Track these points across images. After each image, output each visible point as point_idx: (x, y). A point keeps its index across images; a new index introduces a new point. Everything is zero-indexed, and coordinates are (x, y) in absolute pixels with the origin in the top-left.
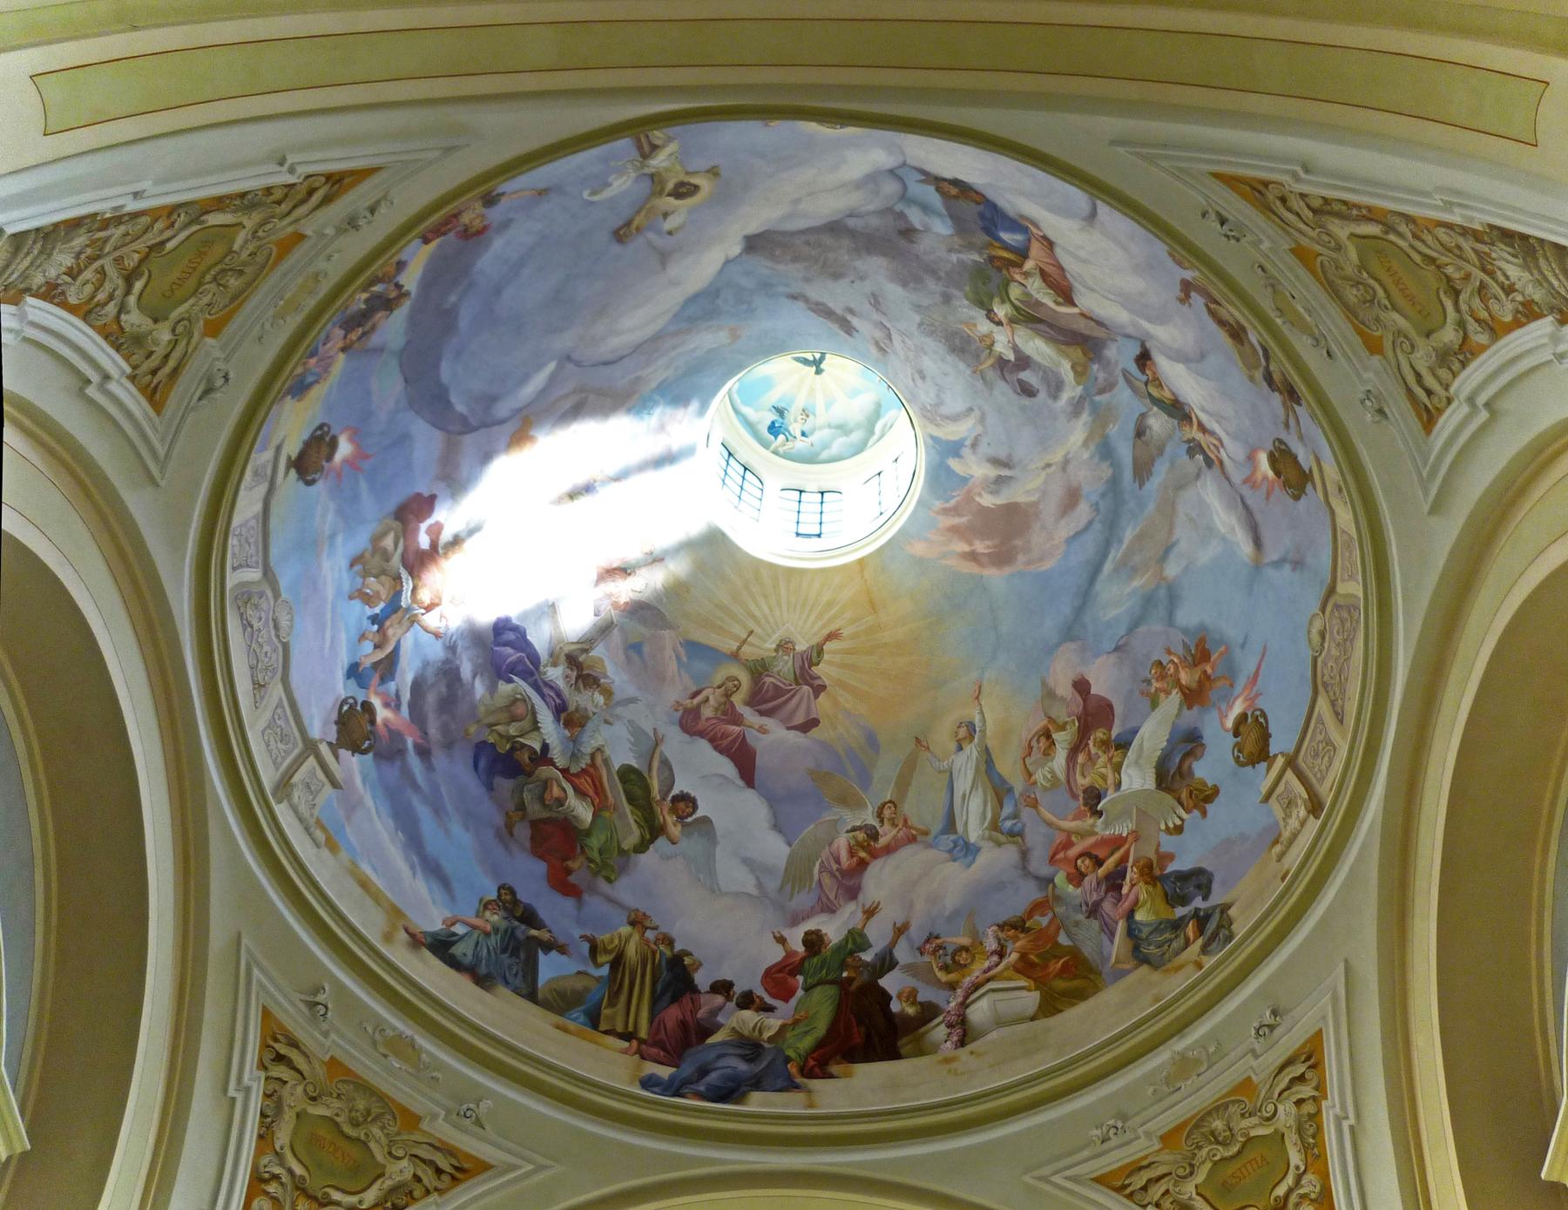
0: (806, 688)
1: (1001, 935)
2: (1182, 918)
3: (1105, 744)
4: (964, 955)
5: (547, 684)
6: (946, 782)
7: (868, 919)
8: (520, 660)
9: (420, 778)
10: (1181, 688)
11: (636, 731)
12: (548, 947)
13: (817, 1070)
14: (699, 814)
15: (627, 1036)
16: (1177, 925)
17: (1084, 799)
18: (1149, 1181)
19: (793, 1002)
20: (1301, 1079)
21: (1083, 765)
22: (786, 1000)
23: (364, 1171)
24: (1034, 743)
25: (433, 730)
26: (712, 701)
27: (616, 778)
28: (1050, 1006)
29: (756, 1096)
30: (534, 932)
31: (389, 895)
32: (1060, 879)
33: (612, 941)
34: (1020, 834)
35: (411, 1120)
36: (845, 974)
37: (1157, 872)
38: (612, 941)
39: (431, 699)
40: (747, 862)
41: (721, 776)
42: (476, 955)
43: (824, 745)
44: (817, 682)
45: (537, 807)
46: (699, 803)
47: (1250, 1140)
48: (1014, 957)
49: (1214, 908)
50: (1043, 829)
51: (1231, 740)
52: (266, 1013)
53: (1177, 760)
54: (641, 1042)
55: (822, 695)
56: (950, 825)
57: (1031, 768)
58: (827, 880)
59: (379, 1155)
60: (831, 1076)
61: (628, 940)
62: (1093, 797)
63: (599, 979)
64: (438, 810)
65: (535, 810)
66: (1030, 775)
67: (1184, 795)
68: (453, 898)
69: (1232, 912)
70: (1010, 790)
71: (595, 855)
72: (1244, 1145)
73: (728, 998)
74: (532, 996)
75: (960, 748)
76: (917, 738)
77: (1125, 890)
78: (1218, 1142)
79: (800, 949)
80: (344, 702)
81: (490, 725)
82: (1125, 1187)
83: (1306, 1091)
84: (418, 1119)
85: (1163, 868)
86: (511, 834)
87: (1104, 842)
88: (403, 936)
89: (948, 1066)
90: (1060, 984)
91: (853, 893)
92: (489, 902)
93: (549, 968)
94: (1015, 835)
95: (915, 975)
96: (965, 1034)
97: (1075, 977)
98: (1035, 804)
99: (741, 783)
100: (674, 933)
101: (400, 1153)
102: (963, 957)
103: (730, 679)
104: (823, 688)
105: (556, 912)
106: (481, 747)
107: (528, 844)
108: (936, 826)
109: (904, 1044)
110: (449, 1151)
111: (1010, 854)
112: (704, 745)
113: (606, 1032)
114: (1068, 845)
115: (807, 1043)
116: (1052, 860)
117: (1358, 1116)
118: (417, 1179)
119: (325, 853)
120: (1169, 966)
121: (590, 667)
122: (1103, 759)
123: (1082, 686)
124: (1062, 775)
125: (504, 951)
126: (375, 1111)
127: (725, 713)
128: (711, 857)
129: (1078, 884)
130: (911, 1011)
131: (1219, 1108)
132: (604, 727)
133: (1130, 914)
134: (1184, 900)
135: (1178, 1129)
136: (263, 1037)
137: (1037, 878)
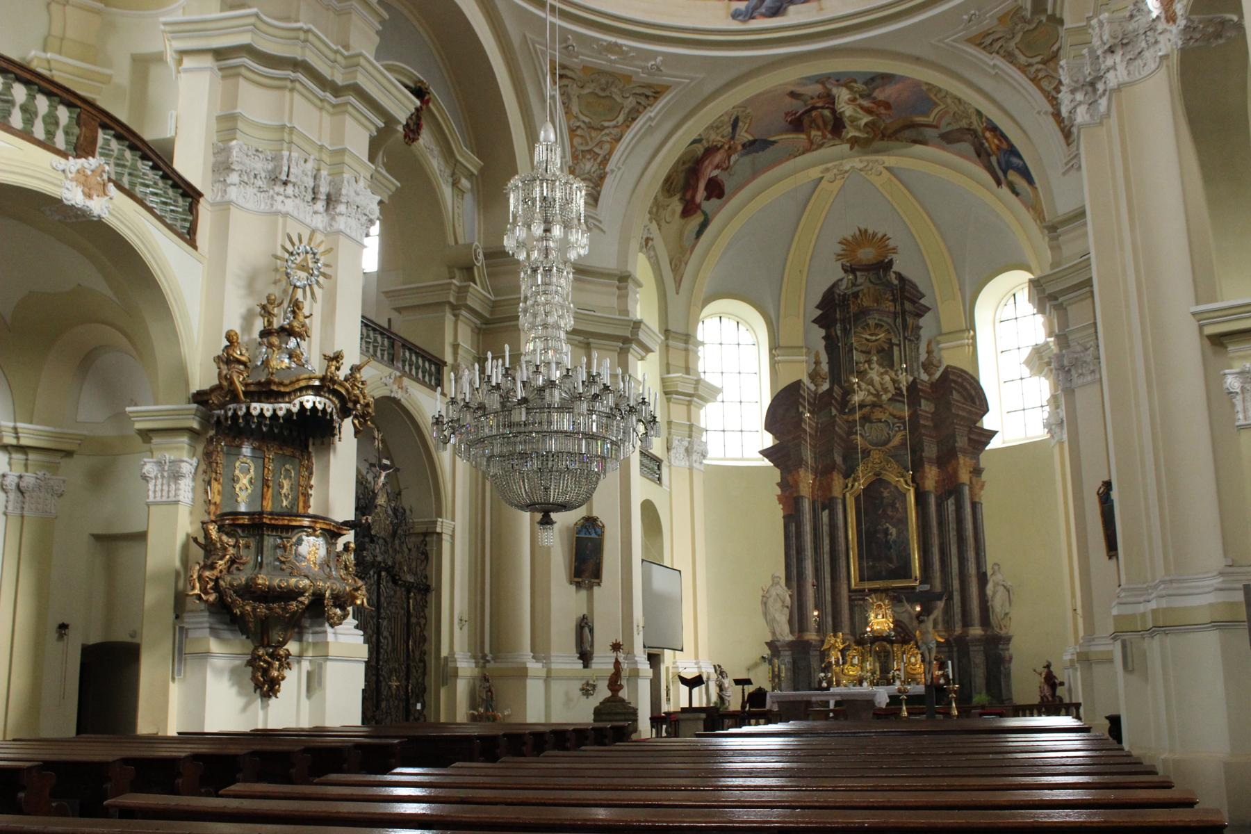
23: (614, 109)
29: (792, 9)
35: (627, 78)
59: (619, 99)
78: (1025, 22)
84: (631, 77)
101: (628, 95)
110: (649, 86)
118: (639, 103)
126: (610, 80)
135: (1006, 14)
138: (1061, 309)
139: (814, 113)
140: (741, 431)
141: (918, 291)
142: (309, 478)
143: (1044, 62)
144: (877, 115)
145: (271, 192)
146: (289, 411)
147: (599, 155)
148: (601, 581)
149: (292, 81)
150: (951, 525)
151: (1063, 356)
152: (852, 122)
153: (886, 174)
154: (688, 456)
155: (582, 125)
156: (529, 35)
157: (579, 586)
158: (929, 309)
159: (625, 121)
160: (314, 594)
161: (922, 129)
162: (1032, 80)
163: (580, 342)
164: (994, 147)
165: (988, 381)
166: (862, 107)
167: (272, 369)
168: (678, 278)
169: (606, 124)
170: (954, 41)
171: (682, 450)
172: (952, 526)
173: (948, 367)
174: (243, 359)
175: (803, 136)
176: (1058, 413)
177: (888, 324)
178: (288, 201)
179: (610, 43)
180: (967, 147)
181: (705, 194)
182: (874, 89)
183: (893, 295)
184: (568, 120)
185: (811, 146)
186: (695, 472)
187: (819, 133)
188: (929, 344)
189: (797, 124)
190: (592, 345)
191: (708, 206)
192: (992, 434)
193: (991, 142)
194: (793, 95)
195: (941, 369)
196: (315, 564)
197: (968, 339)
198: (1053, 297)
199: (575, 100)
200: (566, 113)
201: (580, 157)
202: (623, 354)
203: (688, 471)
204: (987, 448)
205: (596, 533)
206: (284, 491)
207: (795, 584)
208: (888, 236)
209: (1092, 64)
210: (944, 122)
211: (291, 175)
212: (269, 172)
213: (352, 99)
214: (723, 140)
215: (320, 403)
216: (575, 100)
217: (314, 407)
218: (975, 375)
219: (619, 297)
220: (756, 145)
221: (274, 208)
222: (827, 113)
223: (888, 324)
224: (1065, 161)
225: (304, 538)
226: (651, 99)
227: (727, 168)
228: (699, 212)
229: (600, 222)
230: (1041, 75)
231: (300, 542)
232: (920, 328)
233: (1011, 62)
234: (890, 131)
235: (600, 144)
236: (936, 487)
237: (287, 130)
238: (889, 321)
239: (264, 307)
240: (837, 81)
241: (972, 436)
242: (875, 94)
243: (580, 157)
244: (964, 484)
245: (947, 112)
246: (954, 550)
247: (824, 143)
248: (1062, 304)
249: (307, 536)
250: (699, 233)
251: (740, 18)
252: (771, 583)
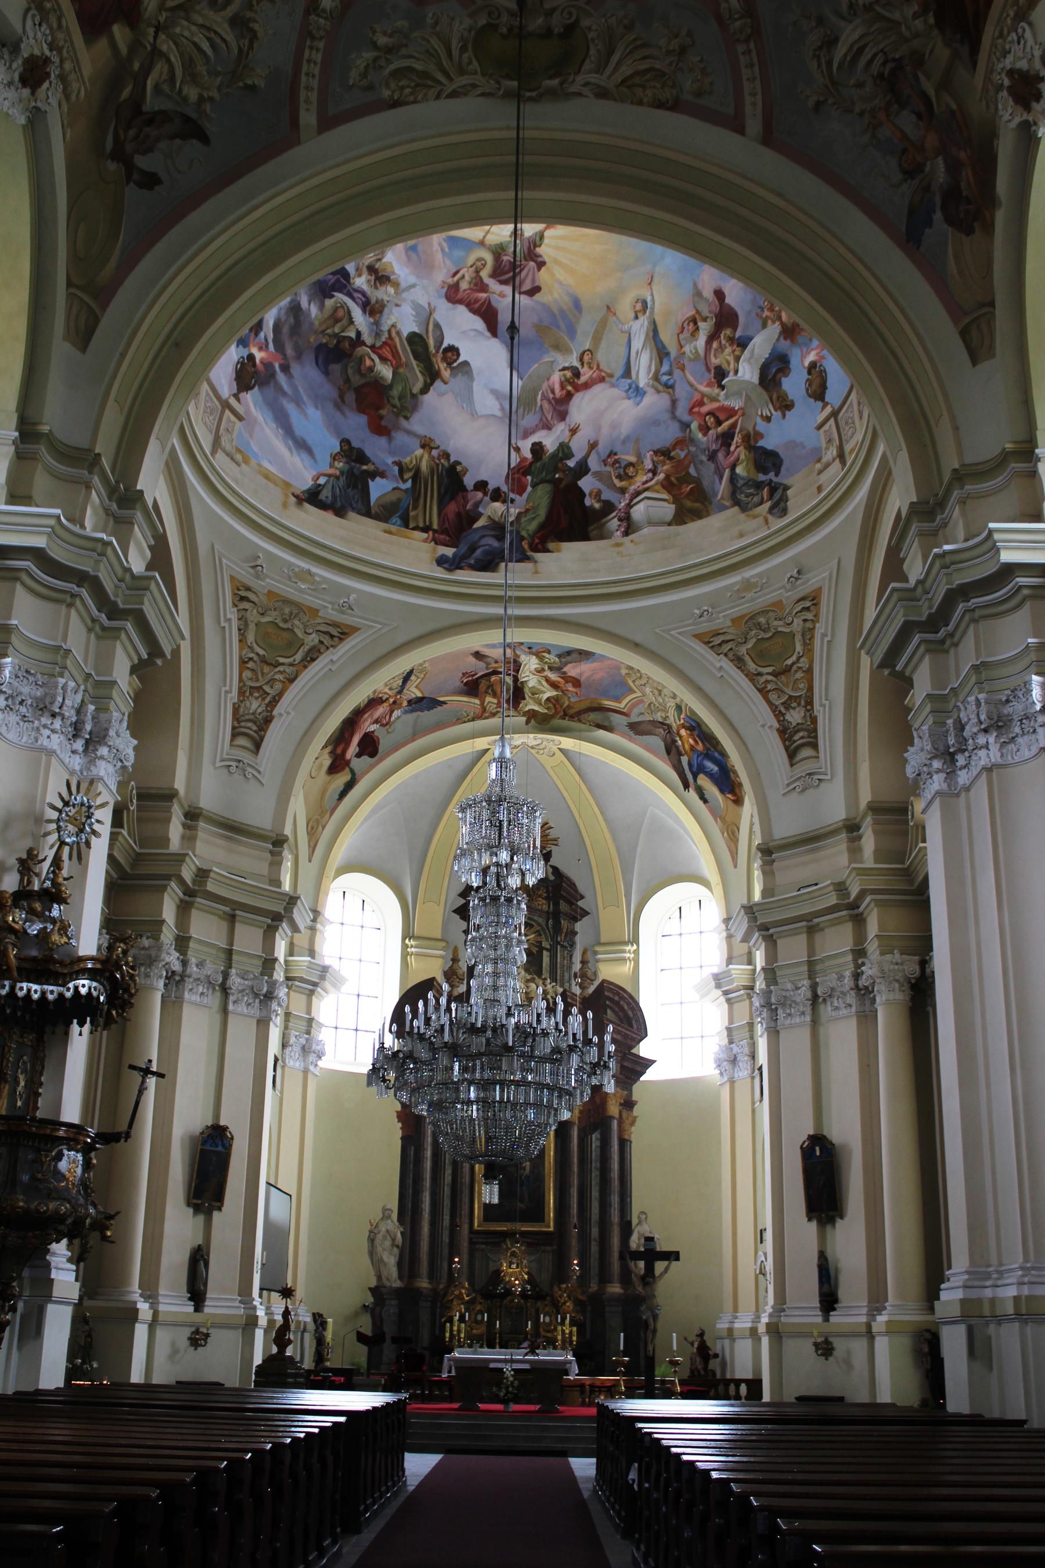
0: (532, 264)
1: (655, 459)
2: (762, 482)
3: (731, 340)
4: (631, 469)
5: (356, 291)
6: (626, 340)
7: (572, 435)
8: (338, 280)
9: (285, 387)
10: (782, 324)
11: (417, 307)
12: (374, 475)
13: (540, 546)
14: (461, 359)
15: (425, 529)
16: (759, 486)
17: (715, 374)
18: (723, 642)
19: (525, 495)
20: (807, 609)
21: (716, 350)
22: (520, 494)
24: (685, 325)
25: (289, 351)
26: (467, 278)
27: (406, 343)
28: (681, 518)
30: (365, 467)
31: (280, 475)
32: (694, 426)
33: (411, 462)
34: (672, 387)
35: (314, 612)
36: (557, 476)
37: (752, 443)
38: (411, 462)
39: (286, 330)
40: (495, 393)
41: (476, 330)
42: (334, 495)
43: (546, 307)
44: (540, 259)
45: (357, 377)
46: (461, 352)
47: (777, 633)
48: (661, 476)
49: (781, 484)
50: (688, 388)
51: (805, 376)
52: (232, 578)
53: (774, 370)
54: (435, 531)
55: (543, 269)
56: (627, 373)
57: (683, 343)
58: (546, 405)
60: (548, 551)
61: (421, 458)
62: (720, 374)
63: (406, 491)
64: (298, 402)
65: (356, 380)
66: (681, 347)
67: (775, 397)
68: (315, 461)
69: (789, 492)
70: (668, 354)
71: (397, 402)
72: (774, 634)
73: (485, 494)
74: (368, 513)
75: (637, 318)
76: (608, 308)
77: (732, 448)
79: (529, 455)
80: (238, 363)
81: (323, 332)
82: (709, 642)
83: (809, 616)
84: (318, 611)
85: (756, 442)
86: (343, 401)
87: (723, 409)
88: (293, 499)
89: (617, 549)
90: (688, 504)
91: (563, 416)
92: (336, 455)
93: (378, 489)
94: (669, 387)
95: (600, 480)
96: (629, 527)
97: (696, 501)
98: (683, 368)
99: (488, 334)
100: (449, 451)
101: (311, 631)
102: (631, 471)
103: (479, 259)
104: (543, 264)
105: (378, 450)
106: (320, 349)
107: (354, 406)
108: (619, 371)
109: (592, 530)
110: (335, 625)
111: (664, 400)
112: (462, 309)
113: (413, 529)
114: (701, 403)
115: (533, 526)
116: (691, 412)
117: (833, 636)
118: (321, 642)
119: (243, 466)
120: (751, 513)
121: (384, 270)
122: (728, 350)
123: (719, 294)
124: (701, 352)
125: (348, 487)
126: (295, 611)
127: (476, 285)
128: (470, 390)
129: (705, 434)
130: (597, 506)
131: (763, 612)
132: (395, 309)
133: (733, 467)
134: (766, 473)
136: (233, 591)
137: (681, 422)
138: (771, 942)
139: (493, 678)
140: (356, 1030)
141: (576, 890)
142: (41, 1074)
143: (775, 674)
144: (563, 691)
145: (36, 723)
146: (61, 995)
147: (268, 694)
148: (222, 1205)
149: (73, 596)
150: (593, 1165)
151: (771, 992)
152: (533, 694)
153: (559, 755)
154: (304, 1056)
155: (256, 658)
156: (216, 547)
157: (197, 1209)
158: (588, 913)
159: (302, 660)
160: (74, 1223)
161: (610, 713)
162: (760, 690)
163: (225, 913)
164: (687, 747)
165: (647, 1003)
166: (547, 680)
167: (53, 943)
168: (312, 844)
169: (282, 660)
170: (679, 633)
171: (297, 1049)
172: (595, 1164)
173: (604, 981)
174: (17, 927)
175: (477, 701)
176: (732, 1049)
177: (539, 924)
178: (54, 736)
179: (302, 570)
180: (657, 742)
181: (358, 749)
182: (566, 664)
183: (547, 892)
184: (241, 649)
185: (483, 714)
186: (310, 1076)
187: (495, 701)
188: (584, 953)
189: (472, 687)
190: (238, 918)
191: (357, 764)
192: (648, 1063)
193: (686, 740)
194: (478, 655)
195: (596, 983)
196: (73, 1184)
197: (629, 952)
198: (764, 928)
199: (252, 627)
200: (240, 641)
201: (247, 694)
202: (270, 932)
203: (301, 1075)
204: (642, 1079)
205: (223, 1145)
206: (20, 1089)
207: (408, 1219)
208: (551, 824)
209: (956, 736)
210: (636, 711)
211: (65, 708)
212: (36, 698)
213: (129, 626)
214: (390, 693)
215: (95, 988)
216: (252, 627)
217: (89, 993)
218: (633, 994)
219: (271, 864)
220: (421, 703)
221: (39, 742)
222: (509, 680)
223: (539, 924)
224: (786, 782)
225: (66, 1152)
226: (336, 639)
227: (387, 724)
228: (347, 769)
229: (259, 772)
230: (769, 687)
231: (60, 1156)
232: (576, 933)
233: (739, 668)
234: (572, 712)
235: (271, 682)
236: (579, 1118)
237: (62, 652)
238: (540, 920)
239: (21, 861)
240: (530, 648)
241: (626, 1064)
242: (565, 669)
243: (247, 694)
244: (612, 1118)
245: (642, 701)
246: (595, 1193)
247: (498, 712)
248: (772, 936)
249: (69, 1150)
250: (343, 794)
251: (446, 565)
252: (381, 1216)
